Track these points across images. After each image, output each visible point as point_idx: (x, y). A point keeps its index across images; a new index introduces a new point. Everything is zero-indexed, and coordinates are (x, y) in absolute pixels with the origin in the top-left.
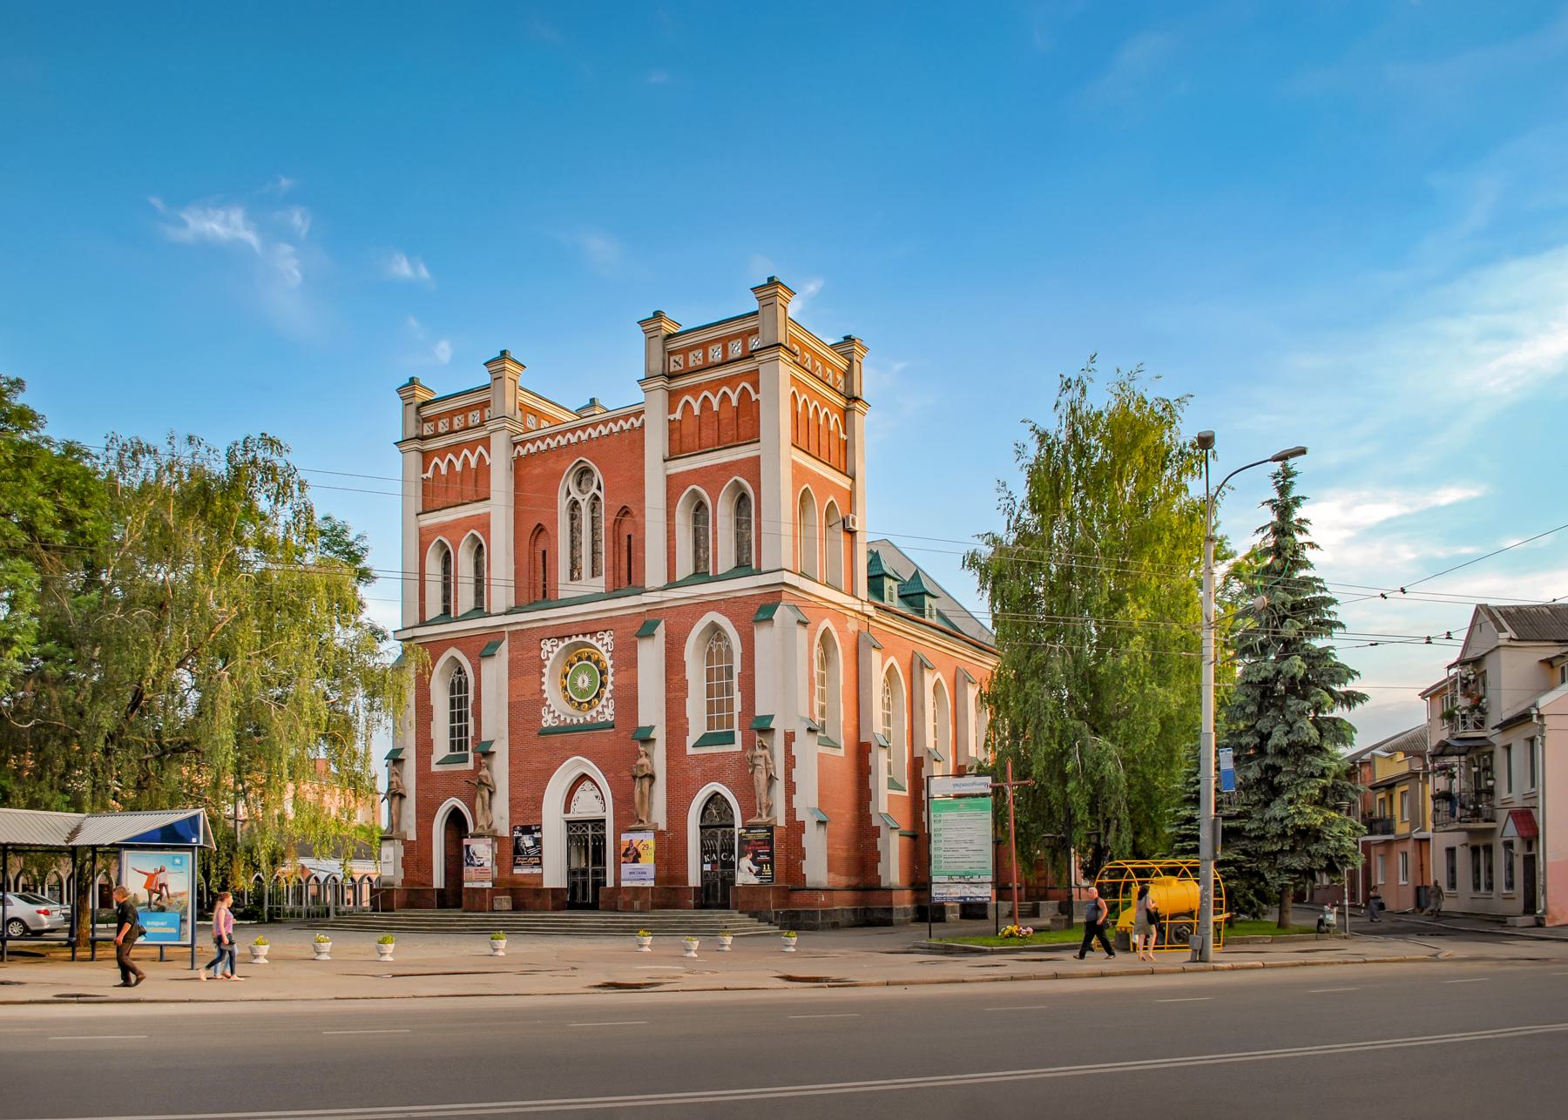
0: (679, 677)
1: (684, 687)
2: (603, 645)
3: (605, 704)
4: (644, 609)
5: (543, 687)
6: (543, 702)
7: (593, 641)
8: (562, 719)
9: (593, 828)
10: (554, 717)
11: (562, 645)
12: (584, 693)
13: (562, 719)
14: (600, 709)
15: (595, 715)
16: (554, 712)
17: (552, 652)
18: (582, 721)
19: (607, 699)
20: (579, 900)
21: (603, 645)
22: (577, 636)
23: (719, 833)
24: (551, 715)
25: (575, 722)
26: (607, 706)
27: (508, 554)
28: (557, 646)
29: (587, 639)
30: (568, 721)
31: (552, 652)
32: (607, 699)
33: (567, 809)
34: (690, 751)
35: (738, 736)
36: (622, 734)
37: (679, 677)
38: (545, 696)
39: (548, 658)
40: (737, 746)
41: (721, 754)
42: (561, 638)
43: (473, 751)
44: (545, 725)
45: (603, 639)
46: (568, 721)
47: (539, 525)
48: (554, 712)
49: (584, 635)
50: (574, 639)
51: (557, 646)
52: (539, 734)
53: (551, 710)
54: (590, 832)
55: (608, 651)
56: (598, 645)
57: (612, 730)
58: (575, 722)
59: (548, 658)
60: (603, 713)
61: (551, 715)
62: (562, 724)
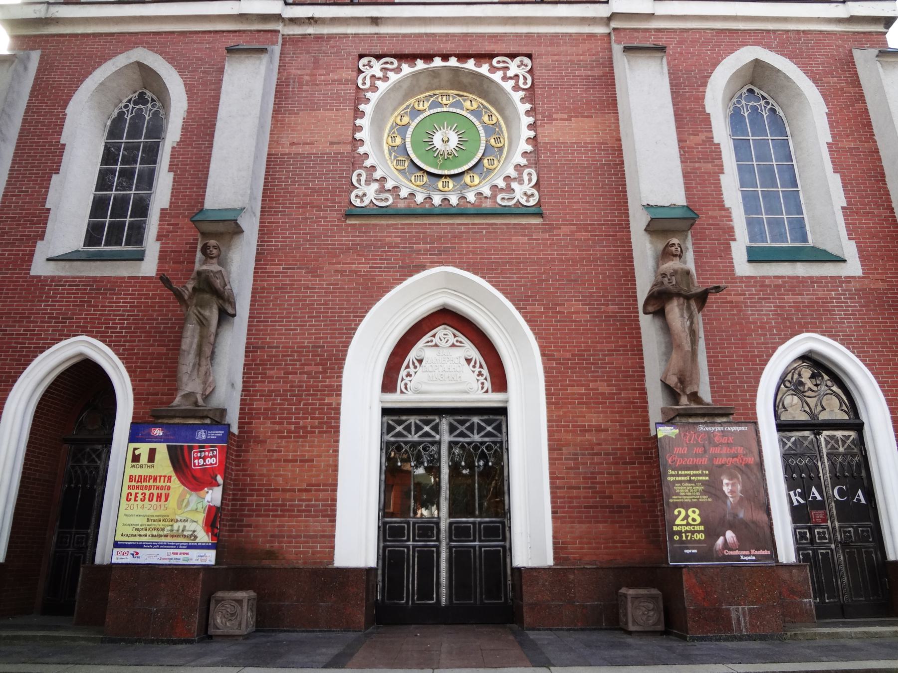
0: (702, 136)
1: (714, 153)
2: (505, 78)
3: (513, 174)
4: (601, 30)
5: (358, 136)
6: (356, 161)
7: (484, 69)
8: (404, 193)
9: (452, 429)
10: (382, 190)
11: (406, 69)
12: (448, 158)
13: (404, 193)
14: (501, 184)
15: (487, 191)
16: (383, 179)
17: (386, 79)
18: (454, 200)
19: (518, 167)
20: (409, 598)
21: (505, 78)
22: (445, 57)
23: (822, 440)
24: (375, 186)
25: (437, 200)
26: (520, 181)
28: (398, 70)
29: (470, 64)
30: (420, 198)
31: (386, 79)
32: (518, 167)
33: (389, 383)
34: (742, 267)
35: (850, 250)
36: (565, 230)
37: (702, 136)
38: (361, 150)
39: (374, 88)
40: (853, 267)
41: (819, 280)
42: (411, 58)
43: (159, 237)
44: (357, 203)
45: (507, 68)
46: (420, 198)
48: (383, 179)
49: (463, 57)
50: (438, 62)
51: (398, 70)
52: (348, 216)
53: (377, 175)
54: (446, 438)
55: (516, 88)
56: (497, 77)
57: (536, 221)
58: (437, 200)
59: (374, 88)
60: (511, 190)
61: (375, 186)
62: (402, 205)
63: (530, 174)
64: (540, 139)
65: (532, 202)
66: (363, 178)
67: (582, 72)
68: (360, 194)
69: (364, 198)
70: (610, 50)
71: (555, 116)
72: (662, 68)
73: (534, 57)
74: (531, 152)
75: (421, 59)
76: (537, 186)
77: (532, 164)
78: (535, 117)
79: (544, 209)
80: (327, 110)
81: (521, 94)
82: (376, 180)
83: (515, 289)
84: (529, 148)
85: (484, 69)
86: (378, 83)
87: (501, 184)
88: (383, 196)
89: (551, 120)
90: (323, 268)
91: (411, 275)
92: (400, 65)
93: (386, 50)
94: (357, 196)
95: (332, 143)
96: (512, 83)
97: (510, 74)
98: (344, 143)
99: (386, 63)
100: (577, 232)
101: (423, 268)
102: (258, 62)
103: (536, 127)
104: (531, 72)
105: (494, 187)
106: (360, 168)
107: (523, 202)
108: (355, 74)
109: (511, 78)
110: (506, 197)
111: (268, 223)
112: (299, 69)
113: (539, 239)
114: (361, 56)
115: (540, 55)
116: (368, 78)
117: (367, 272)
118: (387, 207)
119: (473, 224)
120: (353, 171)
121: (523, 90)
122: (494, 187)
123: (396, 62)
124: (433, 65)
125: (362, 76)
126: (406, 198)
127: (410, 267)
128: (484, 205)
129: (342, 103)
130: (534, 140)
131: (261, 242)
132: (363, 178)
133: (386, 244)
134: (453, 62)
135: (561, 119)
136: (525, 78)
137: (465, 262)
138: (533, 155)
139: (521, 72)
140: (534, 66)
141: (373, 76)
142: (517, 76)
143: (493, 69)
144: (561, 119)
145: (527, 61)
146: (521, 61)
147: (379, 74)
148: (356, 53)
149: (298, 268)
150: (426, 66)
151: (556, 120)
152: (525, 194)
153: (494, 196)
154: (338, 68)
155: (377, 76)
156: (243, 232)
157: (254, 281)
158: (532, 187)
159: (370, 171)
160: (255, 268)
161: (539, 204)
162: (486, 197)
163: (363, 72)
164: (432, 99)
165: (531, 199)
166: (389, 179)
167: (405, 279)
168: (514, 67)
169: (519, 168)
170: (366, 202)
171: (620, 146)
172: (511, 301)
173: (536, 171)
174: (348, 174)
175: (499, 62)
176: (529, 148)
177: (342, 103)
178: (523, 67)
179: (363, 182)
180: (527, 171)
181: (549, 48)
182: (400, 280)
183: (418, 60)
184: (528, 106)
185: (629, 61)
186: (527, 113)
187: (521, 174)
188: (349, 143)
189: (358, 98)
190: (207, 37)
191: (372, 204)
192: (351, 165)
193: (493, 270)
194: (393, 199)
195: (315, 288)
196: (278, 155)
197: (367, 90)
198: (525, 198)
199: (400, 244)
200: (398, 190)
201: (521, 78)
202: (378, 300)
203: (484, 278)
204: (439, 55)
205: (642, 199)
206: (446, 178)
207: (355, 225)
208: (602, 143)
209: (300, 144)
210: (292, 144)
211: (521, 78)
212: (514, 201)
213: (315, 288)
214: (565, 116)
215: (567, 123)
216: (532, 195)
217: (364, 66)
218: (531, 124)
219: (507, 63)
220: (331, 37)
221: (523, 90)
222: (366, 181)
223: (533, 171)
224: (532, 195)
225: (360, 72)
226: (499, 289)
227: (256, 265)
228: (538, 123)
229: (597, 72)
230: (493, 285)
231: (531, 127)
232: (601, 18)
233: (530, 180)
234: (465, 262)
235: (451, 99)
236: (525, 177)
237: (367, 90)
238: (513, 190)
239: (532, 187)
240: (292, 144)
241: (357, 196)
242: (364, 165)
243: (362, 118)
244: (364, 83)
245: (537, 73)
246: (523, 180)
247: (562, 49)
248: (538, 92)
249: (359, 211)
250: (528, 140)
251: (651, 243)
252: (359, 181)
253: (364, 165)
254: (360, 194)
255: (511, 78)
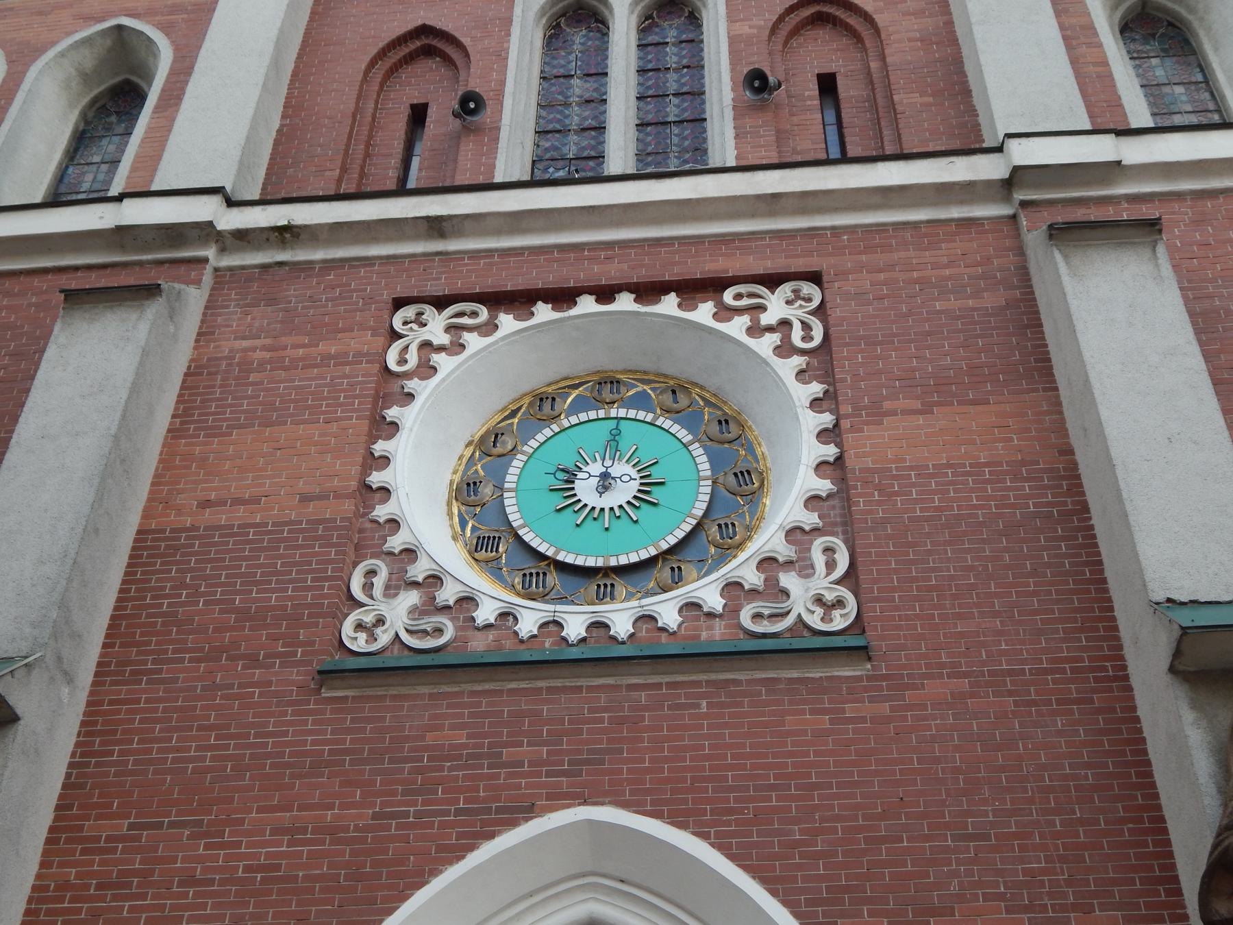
2: (756, 330)
3: (784, 551)
8: (486, 613)
13: (486, 613)
15: (713, 600)
16: (435, 580)
24: (412, 598)
26: (803, 566)
27: (276, 63)
31: (457, 347)
38: (382, 512)
39: (427, 370)
44: (360, 643)
47: (424, 30)
49: (648, 291)
51: (490, 327)
52: (327, 675)
53: (418, 571)
61: (412, 598)
62: (479, 645)
63: (829, 550)
64: (850, 462)
65: (839, 622)
66: (379, 582)
67: (953, 303)
68: (369, 619)
69: (378, 631)
70: (1021, 251)
71: (887, 405)
72: (1157, 266)
73: (825, 278)
74: (829, 496)
75: (546, 302)
76: (850, 578)
77: (834, 524)
78: (835, 411)
79: (872, 636)
80: (305, 422)
81: (798, 361)
82: (415, 584)
83: (799, 867)
84: (824, 486)
85: (704, 313)
86: (438, 359)
87: (752, 578)
88: (428, 623)
89: (877, 414)
90: (241, 822)
91: (491, 836)
92: (493, 317)
93: (460, 286)
94: (360, 626)
95: (305, 499)
96: (774, 339)
97: (767, 319)
98: (337, 497)
99: (461, 314)
100: (973, 695)
101: (528, 811)
102: (134, 316)
103: (839, 435)
104: (820, 311)
105: (732, 588)
106: (375, 556)
107: (815, 621)
108: (381, 341)
109: (770, 329)
110: (766, 612)
111: (111, 702)
112: (244, 338)
113: (863, 720)
114: (399, 303)
115: (842, 274)
116: (413, 349)
117: (366, 829)
118: (437, 650)
119: (671, 685)
120: (355, 565)
121: (803, 352)
122: (732, 588)
123: (484, 314)
124: (574, 312)
125: (397, 346)
126: (488, 626)
127: (488, 811)
128: (704, 635)
129: (341, 405)
130: (833, 467)
131: (83, 755)
132: (379, 582)
133: (427, 748)
134: (625, 302)
135: (905, 412)
136: (806, 326)
137: (648, 792)
138: (835, 502)
139: (794, 313)
140: (827, 299)
141: (426, 345)
142: (785, 324)
143: (725, 313)
144: (905, 412)
145: (808, 288)
146: (796, 291)
147: (442, 339)
148: (387, 296)
149: (172, 825)
150: (557, 315)
151: (893, 413)
152: (819, 600)
153: (732, 611)
154: (343, 330)
155: (436, 342)
156: (13, 718)
157: (43, 865)
158: (838, 582)
159: (402, 561)
160: (52, 830)
161: (858, 625)
162: (711, 615)
163: (400, 336)
164: (577, 392)
165: (836, 613)
166: (448, 582)
167: (472, 848)
168: (776, 306)
169: (799, 535)
170: (384, 638)
171: (1074, 466)
172: (785, 903)
173: (846, 542)
174: (341, 570)
175: (738, 296)
176: (824, 486)
177: (341, 405)
178: (800, 302)
179: (378, 590)
180: (819, 543)
181: (864, 257)
182: (458, 853)
183: (540, 303)
184: (816, 388)
185: (1066, 257)
186: (816, 404)
187: (805, 550)
188: (349, 496)
189: (385, 396)
190: (36, 282)
191: (397, 647)
192: (350, 550)
193: (731, 811)
194: (457, 629)
195: (211, 882)
196: (164, 531)
197: (407, 375)
198: (819, 611)
199: (465, 746)
200: (471, 605)
201: (797, 326)
202: (390, 912)
203: (704, 836)
204: (589, 291)
205: (1150, 585)
206: (606, 575)
207: (345, 698)
208: (1023, 463)
209: (225, 504)
210: (205, 504)
211: (797, 326)
212: (789, 621)
213: (211, 882)
214: (918, 405)
215: (921, 420)
216: (840, 603)
217: (405, 323)
218: (826, 430)
219: (760, 297)
220: (330, 265)
221: (803, 352)
222: (387, 587)
223: (838, 542)
224: (840, 603)
225: (395, 336)
226: (746, 868)
227: (56, 819)
228: (845, 424)
229: (992, 300)
230: (732, 857)
231: (824, 435)
232: (988, 183)
233: (831, 565)
234: (648, 792)
235: (623, 389)
236: (819, 559)
237: (407, 375)
238: (786, 593)
239: (838, 582)
240: (205, 504)
241: (360, 626)
242: (386, 547)
243: (390, 437)
244: (402, 361)
245: (835, 313)
246: (812, 567)
247: (896, 256)
248: (841, 352)
249: (363, 663)
250: (821, 467)
251: (1194, 706)
252: (368, 587)
253: (386, 547)
254: (369, 619)
255: (770, 329)
